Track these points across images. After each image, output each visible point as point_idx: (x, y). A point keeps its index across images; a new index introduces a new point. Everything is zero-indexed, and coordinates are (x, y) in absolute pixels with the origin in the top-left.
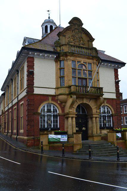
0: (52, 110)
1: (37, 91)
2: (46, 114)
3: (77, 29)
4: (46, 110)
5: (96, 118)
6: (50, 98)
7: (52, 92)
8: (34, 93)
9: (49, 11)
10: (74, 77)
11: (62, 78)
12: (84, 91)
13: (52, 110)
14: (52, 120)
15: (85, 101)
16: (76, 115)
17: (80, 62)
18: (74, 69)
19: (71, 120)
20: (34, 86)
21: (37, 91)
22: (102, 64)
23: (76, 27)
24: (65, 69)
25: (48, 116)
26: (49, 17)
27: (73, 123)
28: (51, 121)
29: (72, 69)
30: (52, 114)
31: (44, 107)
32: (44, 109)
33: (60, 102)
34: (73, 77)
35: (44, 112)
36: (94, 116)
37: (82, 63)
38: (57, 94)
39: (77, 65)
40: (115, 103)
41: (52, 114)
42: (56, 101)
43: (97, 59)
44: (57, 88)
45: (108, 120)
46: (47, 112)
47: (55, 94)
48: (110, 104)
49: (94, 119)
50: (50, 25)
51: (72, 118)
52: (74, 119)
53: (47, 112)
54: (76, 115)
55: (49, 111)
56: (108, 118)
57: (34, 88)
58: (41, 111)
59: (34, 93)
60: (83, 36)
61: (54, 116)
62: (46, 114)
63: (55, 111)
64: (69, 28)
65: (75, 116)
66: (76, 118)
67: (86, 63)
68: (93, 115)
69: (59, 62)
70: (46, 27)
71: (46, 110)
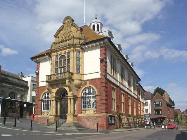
5: (70, 99)
17: (61, 54)
19: (52, 103)
36: (69, 98)
37: (63, 54)
39: (59, 57)
40: (99, 82)
48: (93, 85)
49: (69, 100)
51: (53, 101)
65: (54, 99)
66: (55, 100)
67: (65, 53)
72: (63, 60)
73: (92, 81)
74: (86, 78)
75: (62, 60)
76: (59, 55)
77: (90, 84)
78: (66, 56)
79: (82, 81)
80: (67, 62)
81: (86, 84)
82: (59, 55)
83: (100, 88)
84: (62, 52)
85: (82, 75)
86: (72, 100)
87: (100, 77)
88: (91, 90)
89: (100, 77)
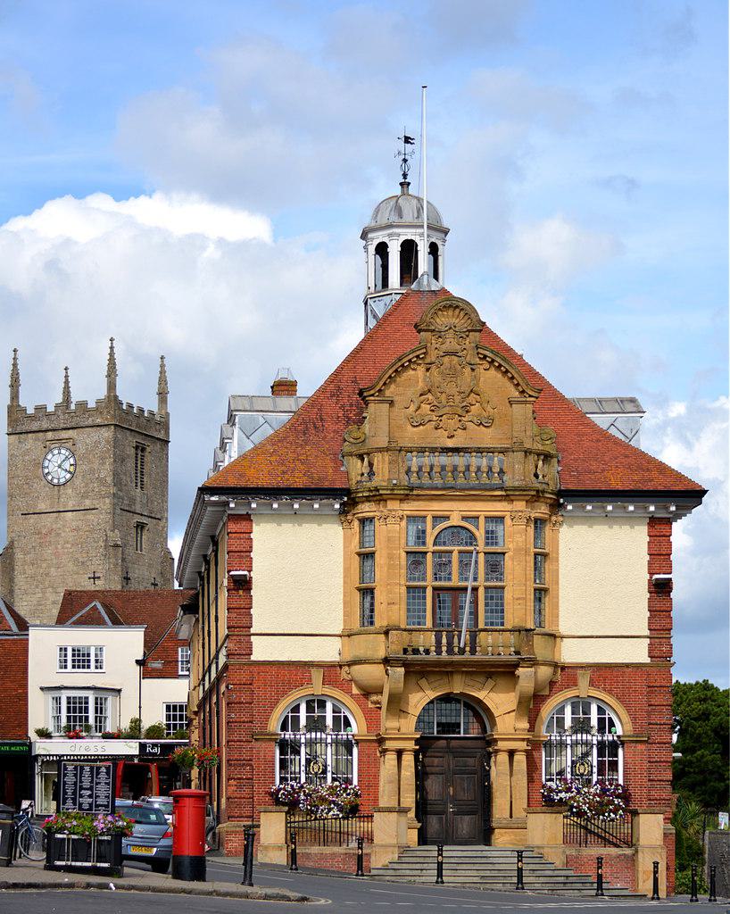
0: (329, 722)
1: (262, 650)
2: (303, 737)
3: (454, 354)
4: (303, 722)
5: (511, 753)
6: (317, 676)
7: (329, 651)
8: (253, 658)
9: (407, 140)
10: (415, 587)
11: (367, 592)
12: (444, 649)
13: (329, 722)
14: (329, 762)
15: (458, 686)
16: (417, 741)
17: (448, 518)
18: (416, 558)
20: (252, 631)
21: (262, 650)
22: (570, 507)
23: (451, 343)
24: (377, 556)
25: (310, 743)
26: (405, 176)
27: (403, 772)
28: (325, 766)
29: (407, 553)
30: (329, 737)
31: (296, 709)
32: (296, 720)
33: (359, 687)
34: (408, 588)
35: (296, 727)
36: (501, 745)
37: (455, 520)
38: (348, 657)
41: (329, 737)
42: (344, 686)
43: (527, 498)
44: (348, 635)
45: (601, 764)
46: (309, 729)
47: (336, 658)
48: (610, 692)
50: (402, 238)
51: (400, 753)
52: (408, 759)
53: (309, 729)
54: (417, 741)
55: (316, 724)
56: (600, 754)
57: (252, 637)
58: (284, 727)
59: (253, 658)
60: (490, 379)
61: (336, 742)
62: (303, 737)
63: (342, 722)
64: (410, 361)
65: (411, 745)
66: (416, 753)
68: (496, 741)
69: (356, 523)
70: (382, 250)
71: (303, 722)
72: (460, 552)
73: (604, 673)
74: (570, 653)
75: (456, 548)
76: (429, 519)
77: (592, 684)
78: (480, 535)
79: (555, 665)
80: (486, 568)
81: (573, 682)
82: (429, 519)
83: (647, 711)
84: (456, 511)
85: (553, 636)
86: (520, 759)
87: (648, 660)
88: (587, 711)
89: (648, 660)
